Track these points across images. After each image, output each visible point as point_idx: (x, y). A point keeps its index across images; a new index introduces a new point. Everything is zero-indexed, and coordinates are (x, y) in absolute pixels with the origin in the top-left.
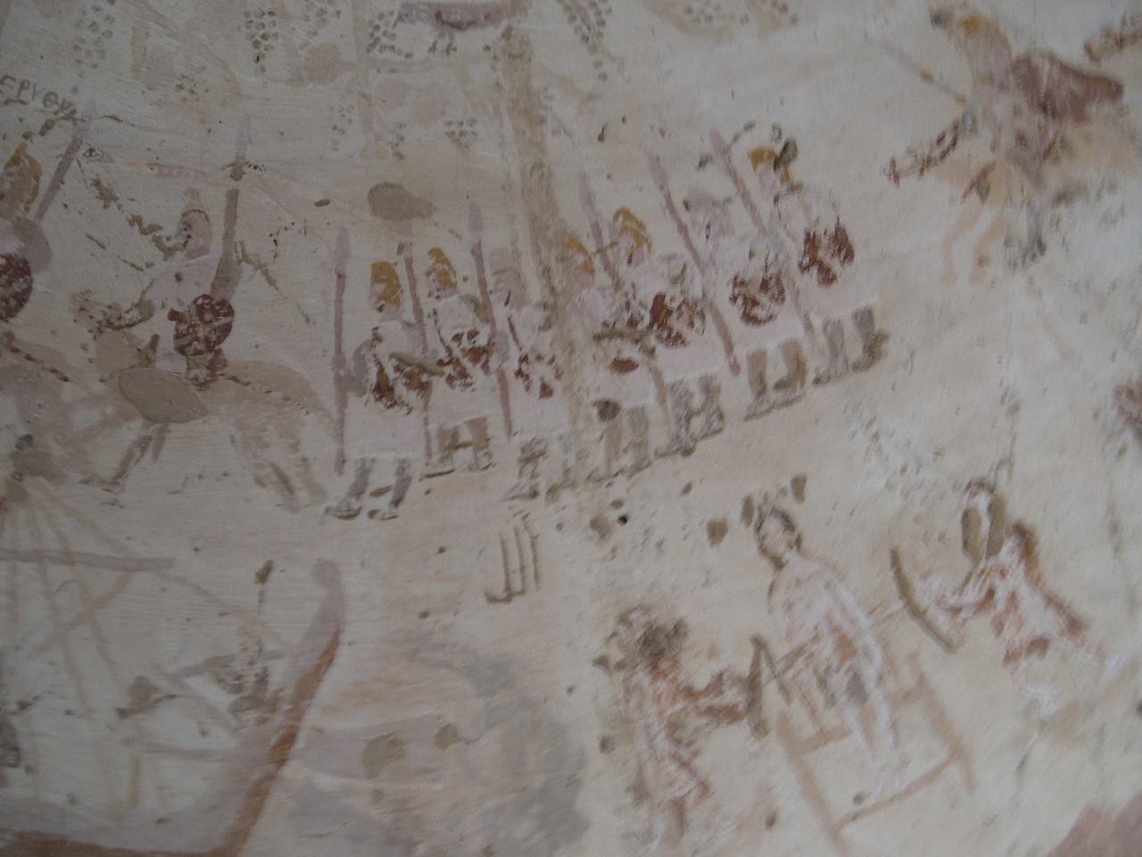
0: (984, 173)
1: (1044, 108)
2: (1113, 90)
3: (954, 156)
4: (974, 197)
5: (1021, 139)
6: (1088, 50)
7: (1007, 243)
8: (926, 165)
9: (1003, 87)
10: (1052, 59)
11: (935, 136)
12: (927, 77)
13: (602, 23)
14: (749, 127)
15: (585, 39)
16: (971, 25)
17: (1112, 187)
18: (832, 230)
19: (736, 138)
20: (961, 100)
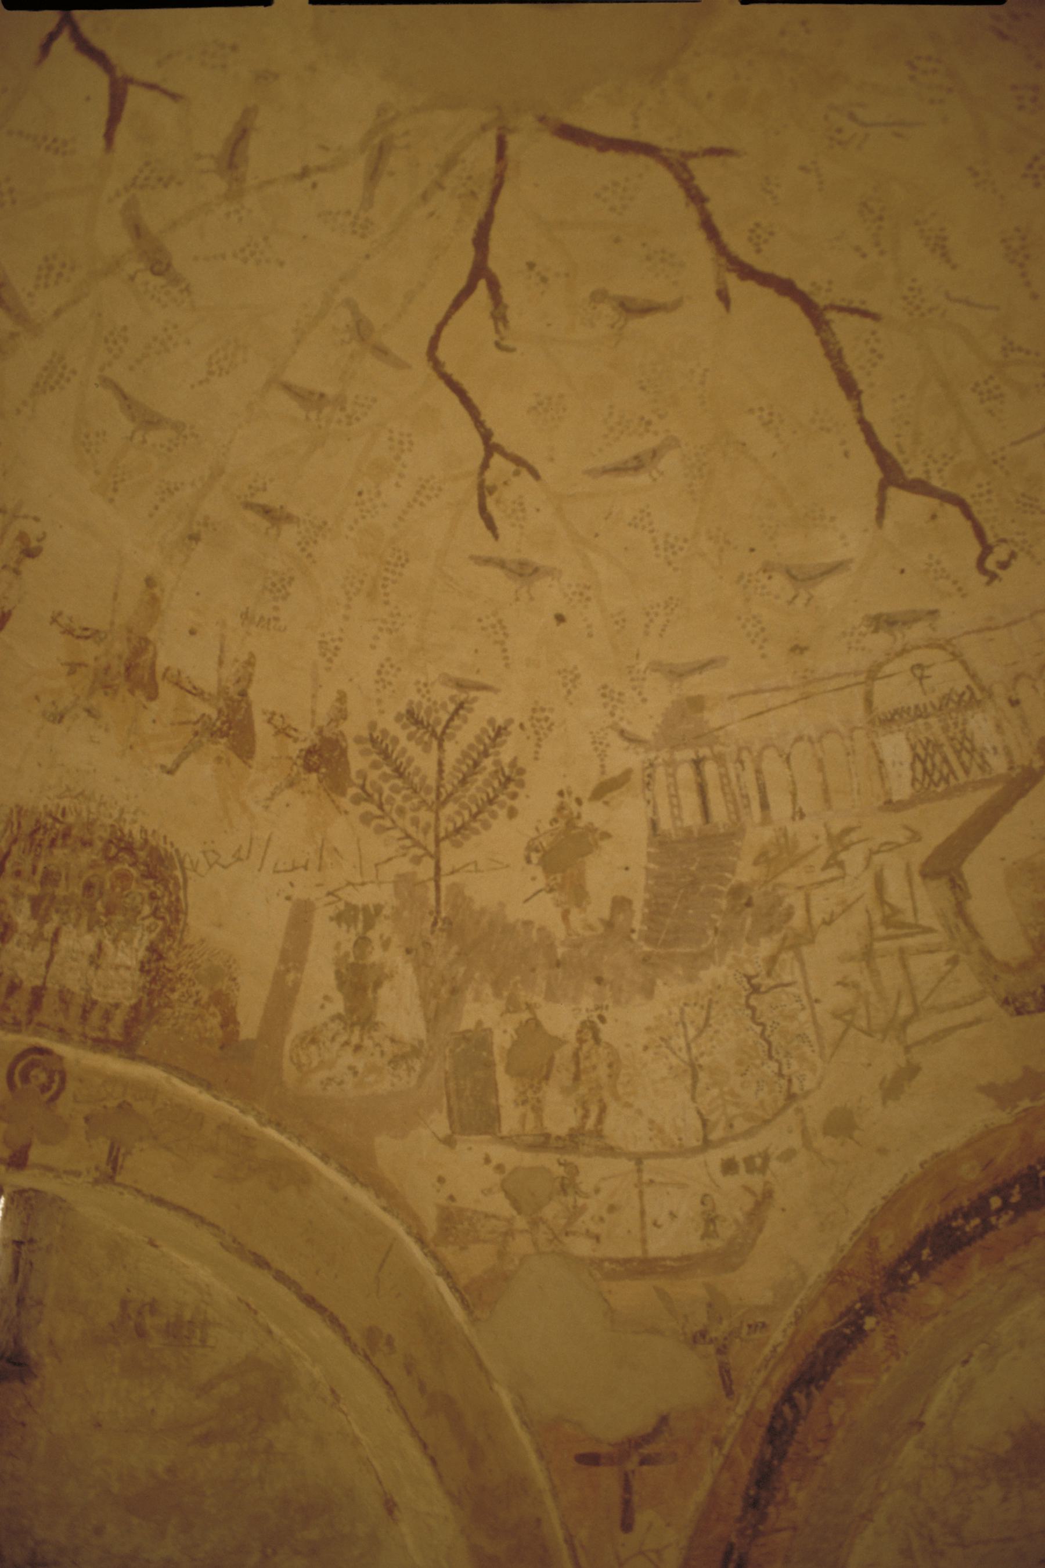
0: (80, 665)
1: (128, 669)
2: (153, 696)
3: (81, 642)
4: (67, 669)
5: (107, 669)
6: (167, 669)
7: (54, 703)
8: (69, 631)
9: (129, 640)
10: (155, 655)
11: (85, 625)
12: (115, 596)
13: (52, 388)
14: (37, 519)
15: (37, 385)
16: (154, 600)
17: (107, 730)
18: (6, 610)
19: (26, 517)
20: (112, 623)
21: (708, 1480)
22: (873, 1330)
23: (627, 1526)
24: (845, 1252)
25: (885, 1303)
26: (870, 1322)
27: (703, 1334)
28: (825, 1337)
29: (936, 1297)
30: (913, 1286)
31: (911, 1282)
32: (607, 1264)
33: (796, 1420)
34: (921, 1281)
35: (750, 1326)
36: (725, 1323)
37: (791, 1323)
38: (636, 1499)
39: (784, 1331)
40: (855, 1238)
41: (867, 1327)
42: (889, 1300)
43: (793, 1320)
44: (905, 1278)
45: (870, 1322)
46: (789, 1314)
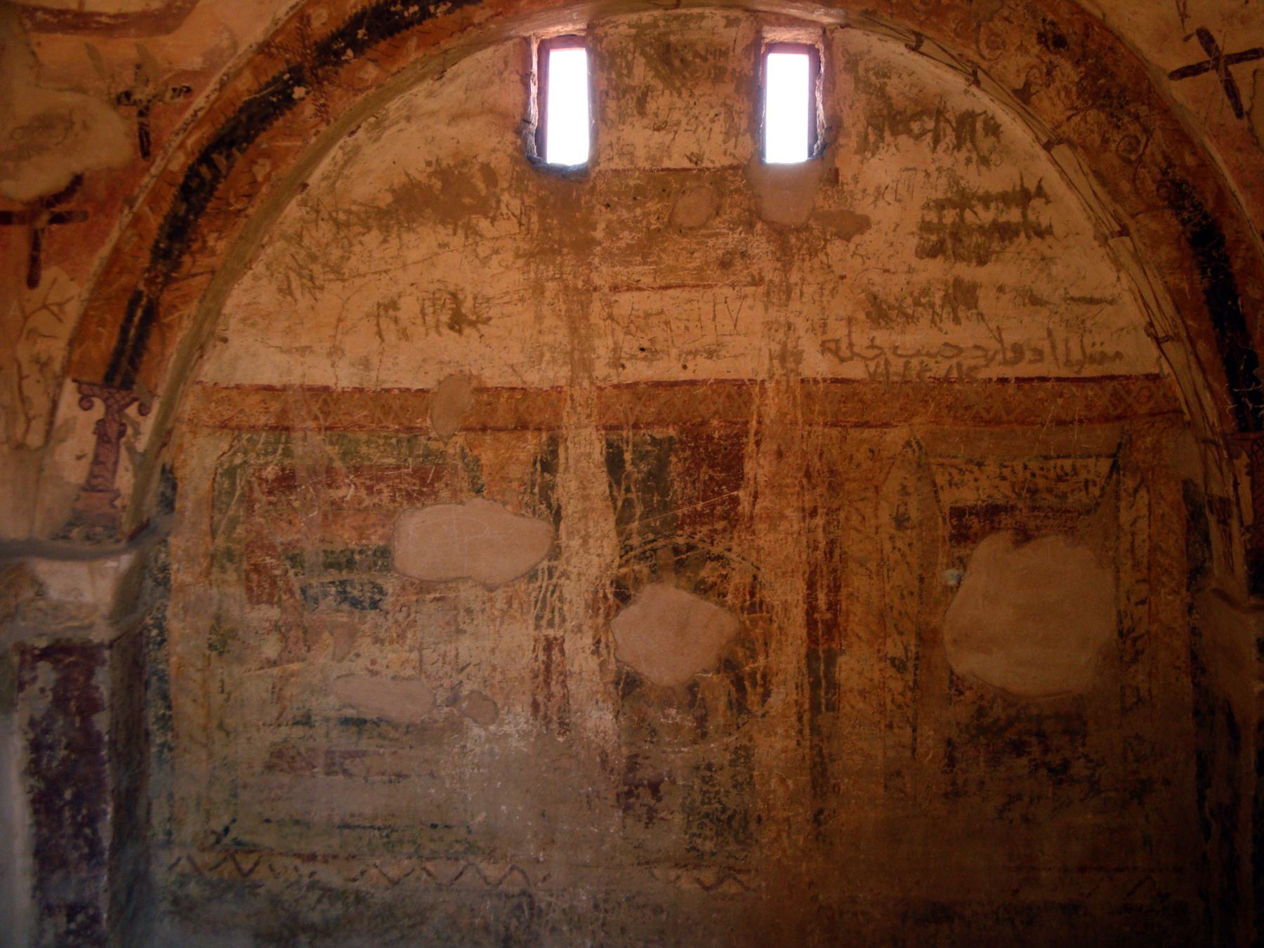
21: (115, 235)
22: (303, 99)
23: (33, 282)
24: (278, 27)
25: (316, 76)
26: (299, 92)
27: (128, 95)
28: (248, 104)
29: (371, 72)
30: (346, 61)
31: (343, 58)
32: (39, 14)
33: (216, 178)
34: (355, 57)
35: (174, 90)
36: (151, 86)
37: (216, 90)
38: (43, 256)
39: (208, 97)
40: (291, 14)
41: (296, 96)
42: (320, 72)
43: (218, 86)
44: (338, 54)
45: (299, 92)
46: (213, 83)
